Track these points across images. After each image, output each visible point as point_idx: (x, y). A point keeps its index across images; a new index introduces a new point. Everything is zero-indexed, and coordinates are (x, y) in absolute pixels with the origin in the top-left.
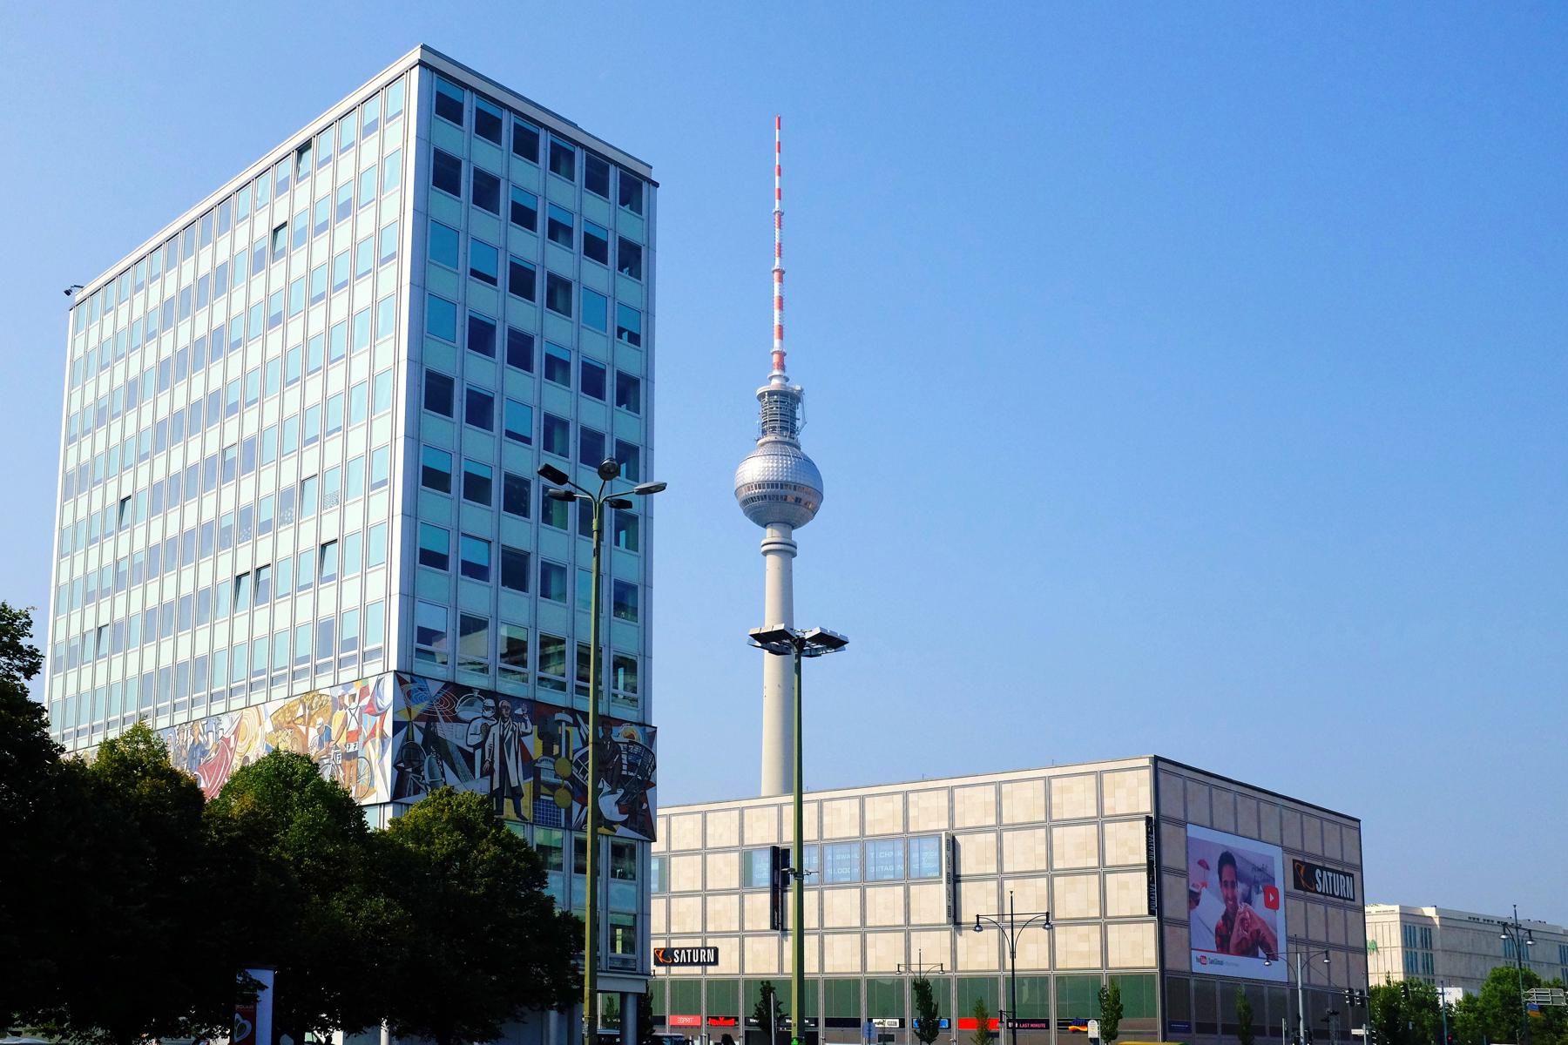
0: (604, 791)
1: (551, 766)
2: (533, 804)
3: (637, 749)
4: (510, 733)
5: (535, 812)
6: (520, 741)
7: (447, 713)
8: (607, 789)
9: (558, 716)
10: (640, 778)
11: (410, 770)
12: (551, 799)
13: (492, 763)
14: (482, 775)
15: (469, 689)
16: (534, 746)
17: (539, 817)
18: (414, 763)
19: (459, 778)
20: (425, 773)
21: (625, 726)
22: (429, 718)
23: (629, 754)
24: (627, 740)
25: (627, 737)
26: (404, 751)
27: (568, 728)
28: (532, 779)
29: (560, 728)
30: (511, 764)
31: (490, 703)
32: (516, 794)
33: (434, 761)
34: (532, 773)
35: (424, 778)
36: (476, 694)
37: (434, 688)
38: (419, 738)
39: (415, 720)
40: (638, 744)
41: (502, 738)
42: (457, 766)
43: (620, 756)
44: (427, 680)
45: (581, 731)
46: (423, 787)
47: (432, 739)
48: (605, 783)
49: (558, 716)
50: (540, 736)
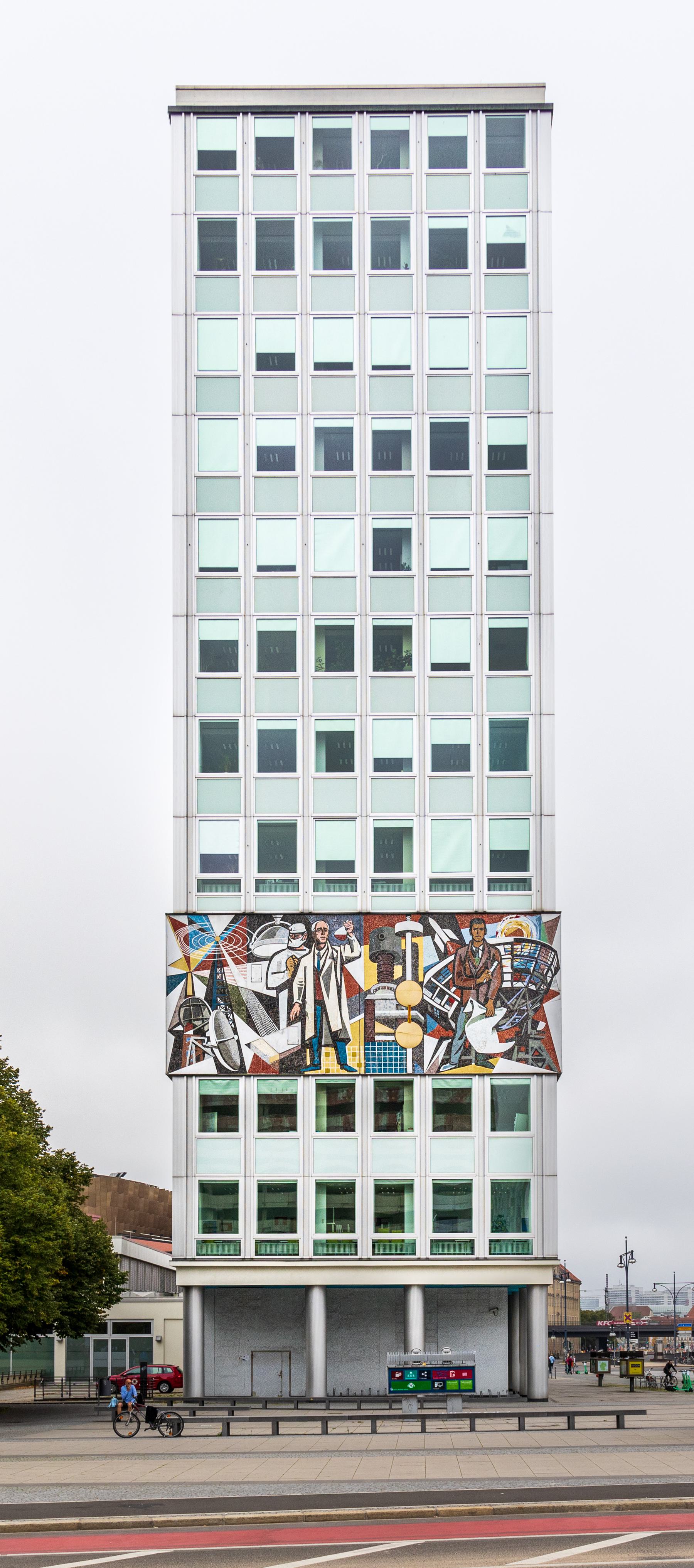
0: (473, 1016)
1: (391, 995)
2: (365, 1049)
3: (527, 949)
4: (329, 962)
6: (343, 969)
7: (238, 953)
8: (478, 1010)
9: (399, 927)
10: (533, 987)
11: (191, 1032)
12: (391, 1038)
13: (303, 1006)
14: (290, 1023)
15: (269, 917)
17: (374, 1065)
18: (196, 1023)
19: (257, 1031)
20: (211, 1033)
22: (216, 963)
23: (514, 957)
24: (511, 939)
25: (510, 935)
26: (183, 1010)
27: (415, 940)
28: (362, 1016)
29: (403, 941)
30: (331, 1002)
31: (299, 928)
32: (339, 1041)
33: (222, 1015)
34: (362, 1007)
35: (209, 1040)
36: (278, 921)
37: (219, 925)
38: (200, 991)
39: (195, 970)
41: (317, 972)
42: (254, 1017)
43: (500, 963)
44: (210, 917)
45: (437, 940)
46: (208, 1050)
48: (475, 1003)
49: (399, 927)
50: (373, 958)
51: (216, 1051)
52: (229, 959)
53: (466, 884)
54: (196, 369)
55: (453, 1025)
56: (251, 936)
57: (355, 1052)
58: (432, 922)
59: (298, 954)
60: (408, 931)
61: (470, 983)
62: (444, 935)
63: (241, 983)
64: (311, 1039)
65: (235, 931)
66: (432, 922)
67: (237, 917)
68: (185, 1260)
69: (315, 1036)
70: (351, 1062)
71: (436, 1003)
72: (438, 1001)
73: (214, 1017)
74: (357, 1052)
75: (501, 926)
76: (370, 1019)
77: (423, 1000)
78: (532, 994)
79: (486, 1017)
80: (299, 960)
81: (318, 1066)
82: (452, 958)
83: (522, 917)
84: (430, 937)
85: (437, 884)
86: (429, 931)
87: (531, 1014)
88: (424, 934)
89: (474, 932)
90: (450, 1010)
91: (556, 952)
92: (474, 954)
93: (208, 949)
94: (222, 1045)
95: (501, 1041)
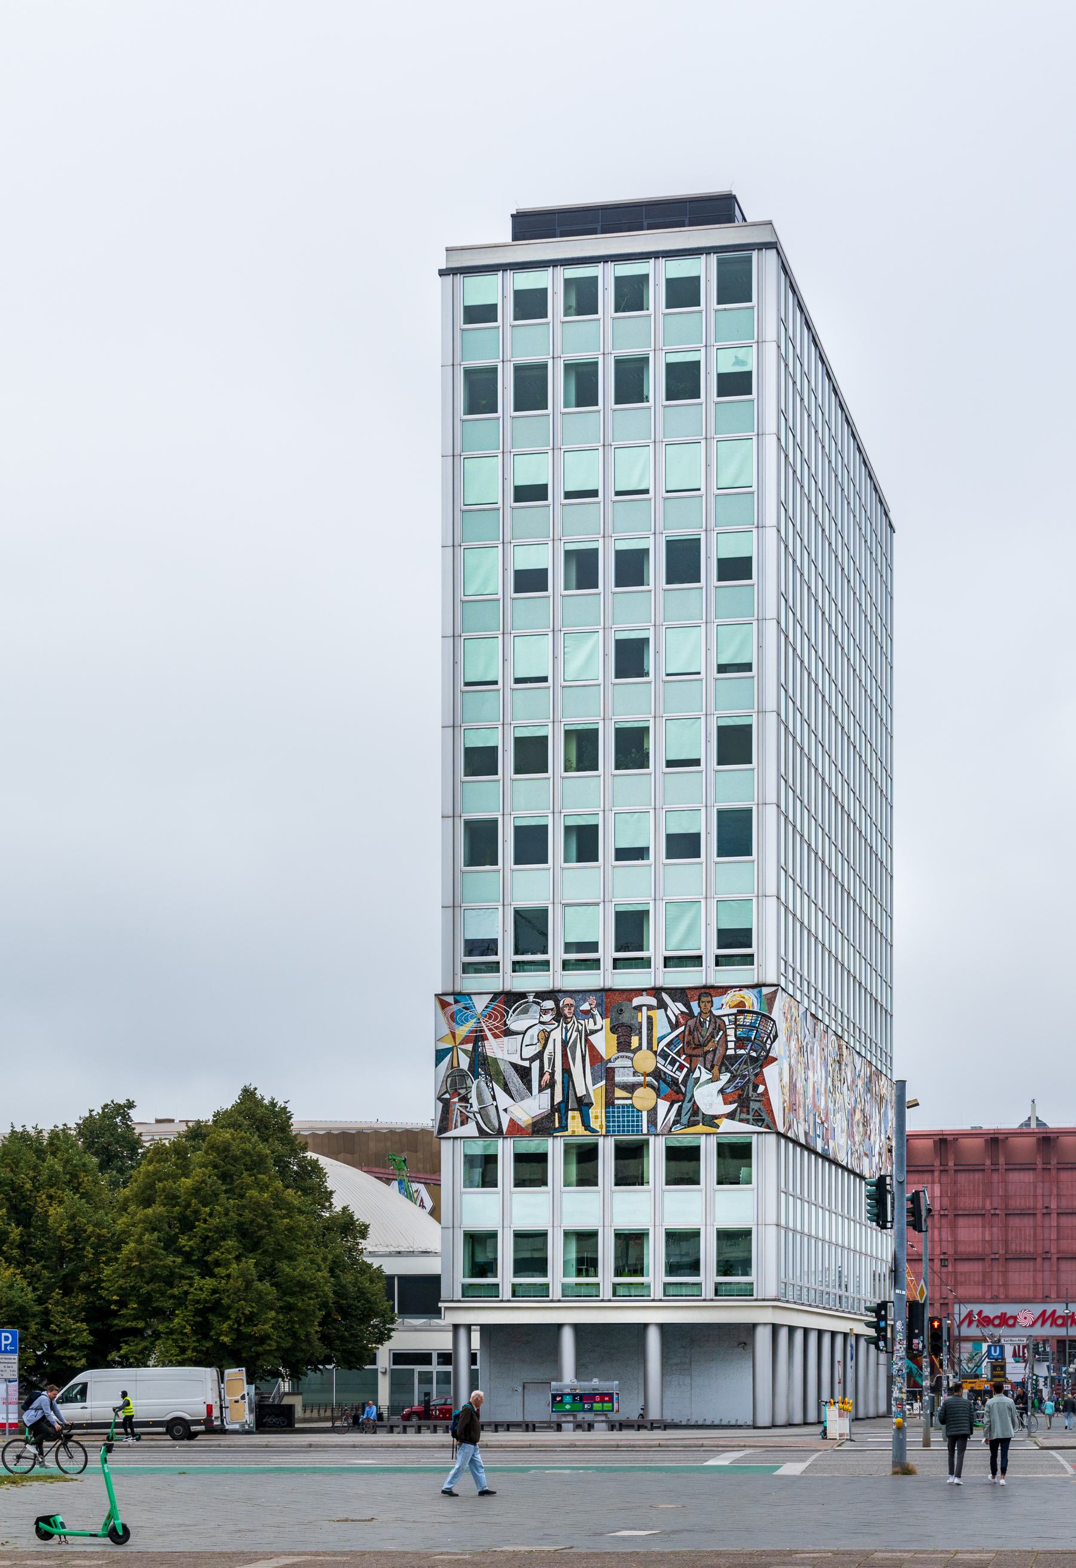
1: (629, 1063)
2: (606, 1112)
3: (749, 1019)
5: (608, 1121)
6: (587, 1040)
7: (497, 1028)
8: (705, 1076)
10: (754, 1054)
11: (456, 1100)
12: (629, 1102)
13: (552, 1074)
14: (541, 1090)
15: (523, 995)
16: (604, 1042)
17: (614, 1126)
18: (461, 1091)
19: (512, 1097)
20: (474, 1100)
21: (731, 993)
22: (477, 1038)
23: (737, 1026)
24: (735, 1011)
25: (733, 1007)
26: (449, 1079)
27: (650, 1013)
28: (604, 1082)
29: (640, 1014)
30: (576, 1070)
31: (549, 1004)
32: (583, 1105)
33: (483, 1084)
34: (604, 1075)
35: (471, 1107)
36: (531, 998)
37: (480, 1003)
38: (464, 1063)
39: (460, 1044)
40: (749, 1012)
41: (565, 1043)
42: (510, 1085)
43: (725, 1032)
44: (472, 996)
45: (669, 1012)
46: (471, 1115)
47: (482, 1064)
48: (703, 1069)
49: (636, 1001)
50: (613, 1029)
51: (478, 1116)
52: (488, 1034)
53: (697, 960)
54: (462, 504)
55: (683, 1089)
56: (508, 1012)
57: (597, 1114)
58: (666, 997)
59: (548, 1028)
60: (644, 1005)
61: (696, 1052)
62: (676, 1008)
63: (499, 1055)
64: (559, 1103)
65: (494, 1009)
66: (666, 997)
67: (496, 996)
68: (452, 1301)
69: (562, 1102)
70: (594, 1124)
71: (668, 1069)
72: (670, 1067)
73: (476, 1086)
74: (599, 1115)
75: (727, 999)
76: (611, 1085)
77: (657, 1067)
78: (754, 1060)
79: (712, 1082)
80: (549, 1033)
81: (564, 1128)
82: (682, 1029)
83: (745, 991)
84: (663, 1010)
85: (668, 961)
86: (662, 1005)
87: (752, 1078)
88: (659, 1008)
89: (702, 1005)
90: (681, 1076)
91: (774, 1021)
92: (702, 1024)
93: (471, 1024)
94: (483, 1111)
95: (725, 1104)
